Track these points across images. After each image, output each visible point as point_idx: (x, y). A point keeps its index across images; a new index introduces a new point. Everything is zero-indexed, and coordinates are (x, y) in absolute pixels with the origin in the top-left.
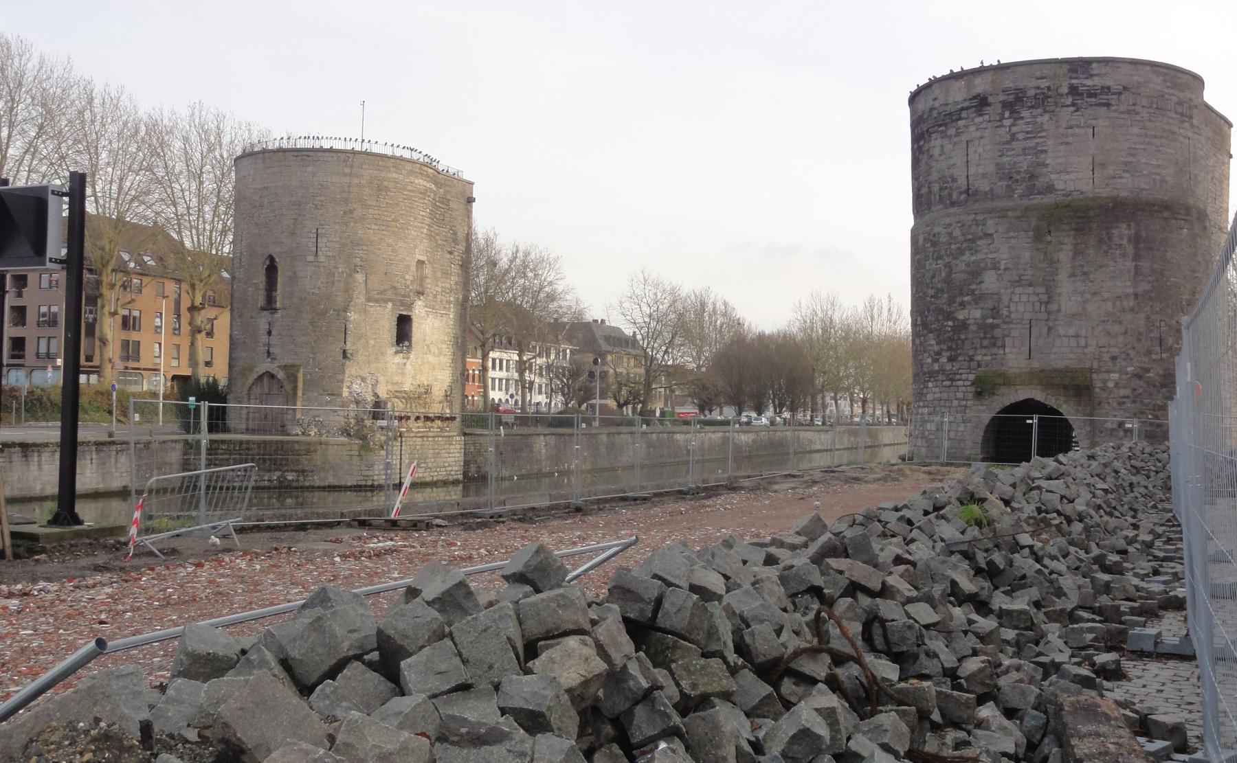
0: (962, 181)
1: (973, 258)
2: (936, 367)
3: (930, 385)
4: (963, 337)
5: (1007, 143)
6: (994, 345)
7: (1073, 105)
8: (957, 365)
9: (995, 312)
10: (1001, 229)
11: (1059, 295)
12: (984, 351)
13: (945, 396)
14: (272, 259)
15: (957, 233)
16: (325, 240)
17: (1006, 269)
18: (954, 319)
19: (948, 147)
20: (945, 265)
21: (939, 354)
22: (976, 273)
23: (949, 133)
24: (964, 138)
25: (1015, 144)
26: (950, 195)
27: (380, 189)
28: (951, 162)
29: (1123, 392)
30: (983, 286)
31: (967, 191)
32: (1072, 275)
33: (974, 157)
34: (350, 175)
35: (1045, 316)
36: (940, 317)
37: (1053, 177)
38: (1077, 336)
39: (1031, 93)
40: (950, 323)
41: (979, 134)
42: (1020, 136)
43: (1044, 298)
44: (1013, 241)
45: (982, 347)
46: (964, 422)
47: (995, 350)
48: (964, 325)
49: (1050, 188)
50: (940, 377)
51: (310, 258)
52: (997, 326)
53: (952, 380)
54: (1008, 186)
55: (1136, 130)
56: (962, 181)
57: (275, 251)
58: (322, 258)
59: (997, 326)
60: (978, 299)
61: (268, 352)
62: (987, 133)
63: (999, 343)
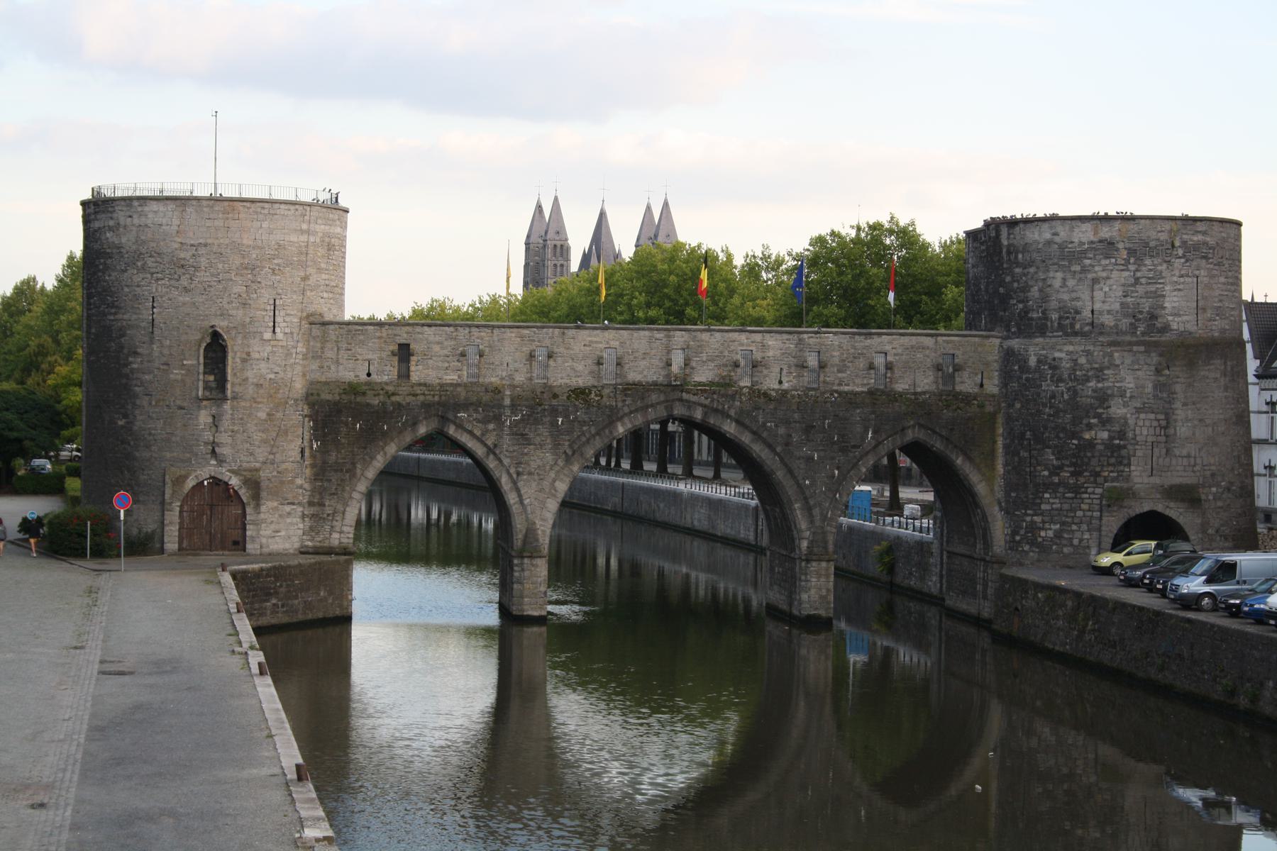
0: (1087, 313)
1: (1100, 385)
2: (1056, 480)
3: (1047, 495)
4: (1089, 454)
5: (1132, 285)
6: (1120, 463)
7: (1184, 256)
8: (1082, 480)
9: (1122, 435)
10: (1128, 361)
11: (1176, 421)
12: (1111, 468)
13: (1066, 506)
14: (216, 335)
15: (1082, 360)
16: (282, 313)
17: (1131, 397)
18: (1080, 438)
19: (1071, 283)
20: (1069, 389)
21: (1061, 468)
22: (1103, 398)
23: (1073, 269)
24: (1090, 276)
25: (1139, 288)
26: (1072, 326)
27: (330, 247)
28: (1074, 295)
29: (1220, 504)
30: (1112, 410)
31: (1092, 324)
32: (1185, 404)
33: (1099, 295)
34: (308, 232)
35: (1163, 439)
36: (1061, 435)
37: (1170, 318)
38: (1189, 456)
39: (1152, 244)
40: (1075, 442)
41: (1104, 274)
42: (1143, 281)
43: (1163, 423)
44: (1139, 373)
45: (1109, 465)
46: (1089, 530)
47: (1121, 468)
48: (1091, 444)
49: (1166, 328)
50: (1061, 490)
51: (268, 335)
52: (1125, 447)
53: (1077, 493)
54: (1131, 324)
55: (1222, 280)
56: (1087, 313)
57: (221, 324)
58: (280, 335)
59: (1125, 447)
60: (1105, 422)
61: (213, 451)
62: (1115, 274)
63: (1126, 462)
